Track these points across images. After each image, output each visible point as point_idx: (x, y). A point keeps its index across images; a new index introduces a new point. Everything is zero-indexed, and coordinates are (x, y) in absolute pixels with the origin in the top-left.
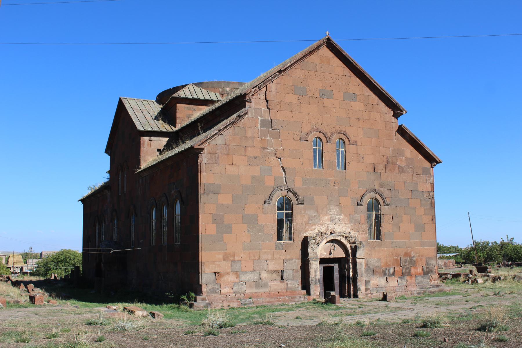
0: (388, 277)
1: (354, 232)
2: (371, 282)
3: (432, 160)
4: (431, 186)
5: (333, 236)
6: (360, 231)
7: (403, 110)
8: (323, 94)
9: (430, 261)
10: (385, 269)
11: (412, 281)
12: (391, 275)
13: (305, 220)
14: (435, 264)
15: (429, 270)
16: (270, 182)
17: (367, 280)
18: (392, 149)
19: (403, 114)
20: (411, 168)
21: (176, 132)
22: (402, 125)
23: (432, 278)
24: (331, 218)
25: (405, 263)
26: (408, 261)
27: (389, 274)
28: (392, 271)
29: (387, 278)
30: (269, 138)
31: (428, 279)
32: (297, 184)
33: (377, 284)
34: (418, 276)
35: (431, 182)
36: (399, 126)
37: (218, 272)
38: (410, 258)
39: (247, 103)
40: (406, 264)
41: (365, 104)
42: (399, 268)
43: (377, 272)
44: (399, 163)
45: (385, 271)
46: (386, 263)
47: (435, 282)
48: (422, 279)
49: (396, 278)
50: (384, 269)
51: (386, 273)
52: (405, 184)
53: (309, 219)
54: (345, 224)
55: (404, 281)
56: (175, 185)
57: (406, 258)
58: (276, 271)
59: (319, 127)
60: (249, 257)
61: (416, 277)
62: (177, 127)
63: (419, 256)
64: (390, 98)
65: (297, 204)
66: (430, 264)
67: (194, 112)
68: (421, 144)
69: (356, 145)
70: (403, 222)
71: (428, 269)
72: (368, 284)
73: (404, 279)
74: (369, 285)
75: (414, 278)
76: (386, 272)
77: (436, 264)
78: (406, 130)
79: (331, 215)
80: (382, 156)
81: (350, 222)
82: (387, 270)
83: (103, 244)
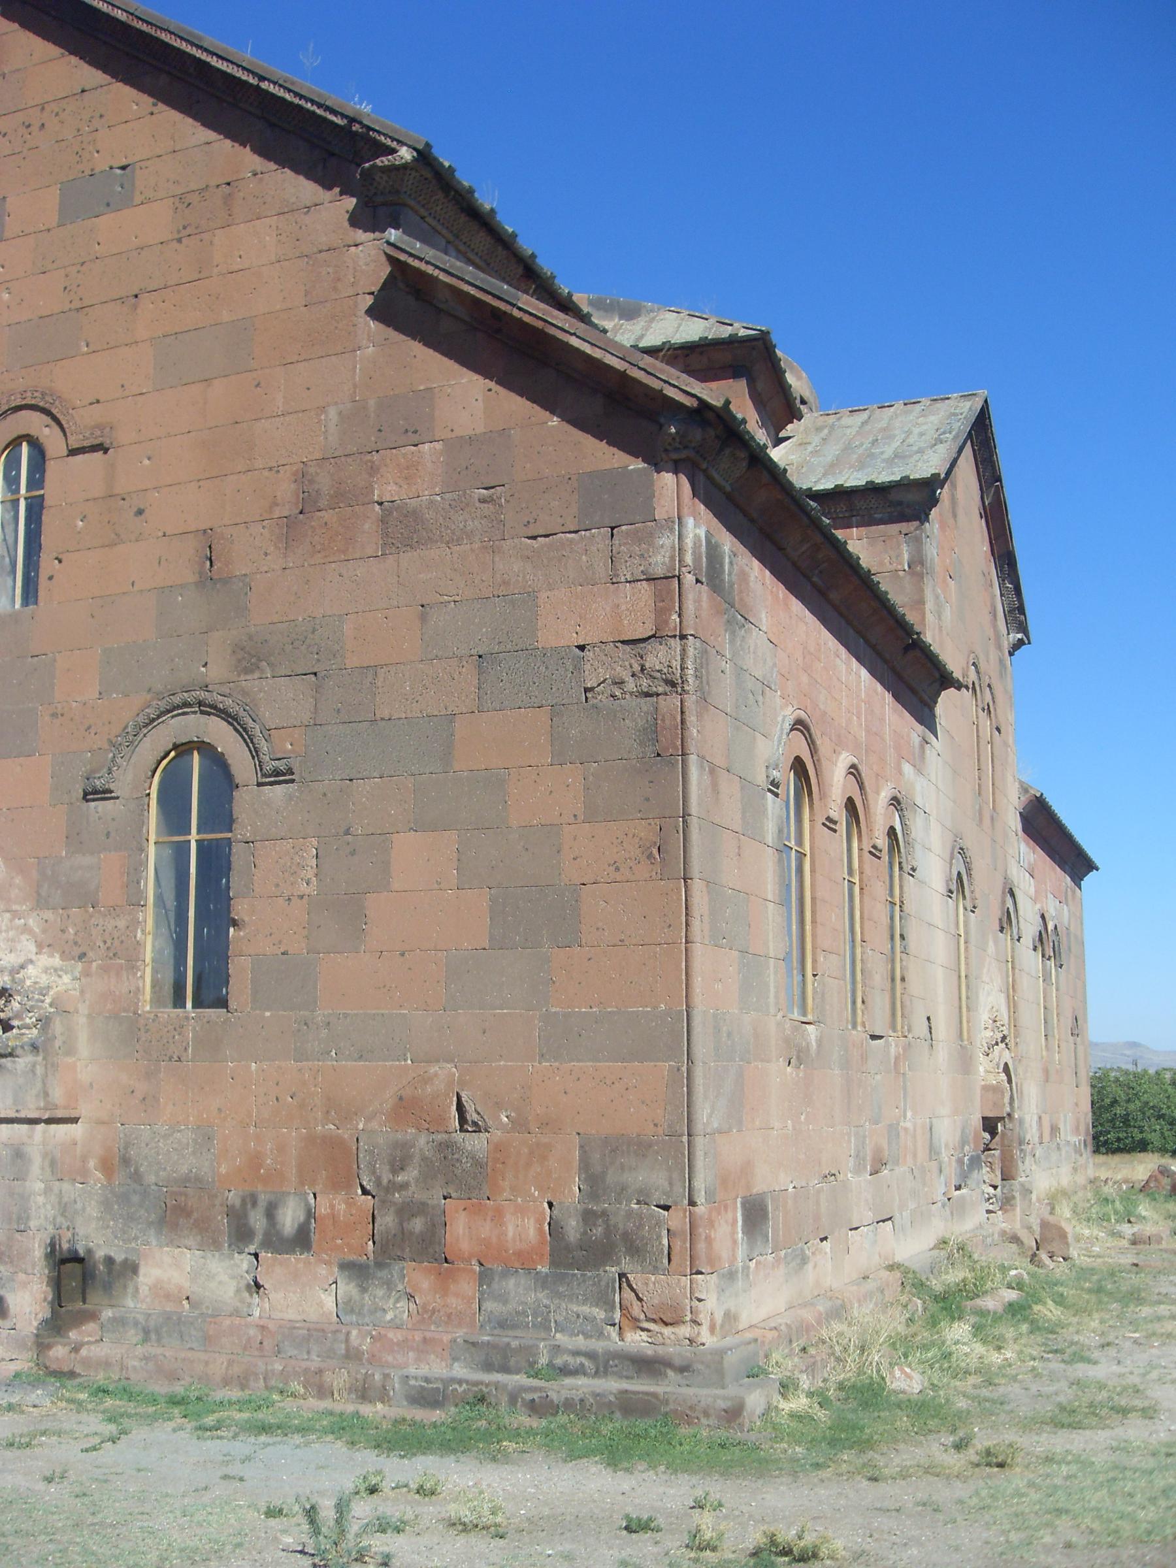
0: (262, 1255)
1: (56, 961)
2: (142, 1270)
4: (659, 597)
6: (91, 954)
7: (394, 145)
9: (622, 1167)
10: (244, 1201)
11: (453, 1301)
12: (282, 1239)
14: (668, 1194)
15: (608, 1232)
17: (119, 1257)
18: (340, 413)
20: (483, 501)
23: (640, 1299)
25: (394, 1171)
26: (416, 1160)
27: (267, 1234)
28: (290, 1218)
29: (256, 1256)
31: (597, 1305)
33: (180, 1289)
34: (505, 1275)
35: (660, 571)
38: (440, 1137)
40: (400, 1178)
42: (350, 1203)
43: (189, 1214)
44: (388, 489)
45: (245, 1216)
46: (255, 1161)
47: (667, 1331)
48: (540, 1295)
49: (322, 1270)
50: (238, 1203)
51: (246, 1225)
52: (423, 618)
54: (8, 915)
55: (380, 1293)
57: (399, 1136)
61: (485, 1277)
63: (519, 1124)
64: (309, 106)
66: (624, 1189)
68: (527, 319)
70: (396, 885)
71: (599, 1231)
72: (125, 1287)
73: (389, 1285)
74: (130, 1290)
75: (467, 1286)
76: (252, 1221)
77: (680, 1191)
78: (410, 261)
80: (266, 473)
81: (38, 901)
82: (254, 1204)
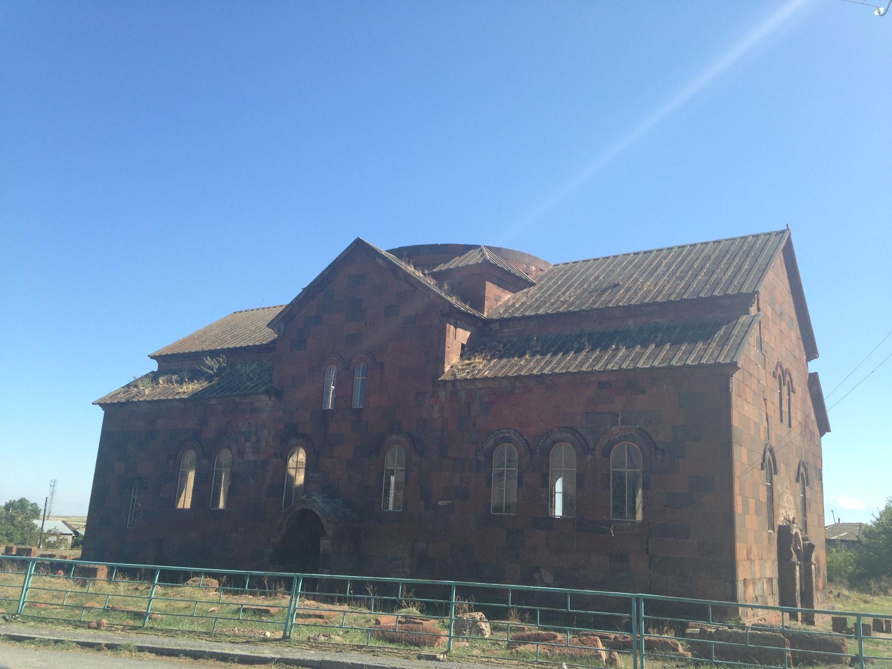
3: (824, 427)
5: (796, 528)
8: (781, 313)
13: (778, 500)
16: (763, 436)
19: (816, 357)
21: (488, 322)
22: (816, 374)
24: (788, 498)
30: (760, 366)
32: (773, 443)
36: (810, 374)
37: (745, 579)
39: (750, 308)
41: (797, 335)
53: (780, 499)
56: (620, 418)
58: (769, 579)
59: (780, 360)
60: (758, 554)
62: (485, 312)
65: (774, 474)
67: (503, 293)
69: (794, 393)
79: (787, 493)
83: (318, 500)
